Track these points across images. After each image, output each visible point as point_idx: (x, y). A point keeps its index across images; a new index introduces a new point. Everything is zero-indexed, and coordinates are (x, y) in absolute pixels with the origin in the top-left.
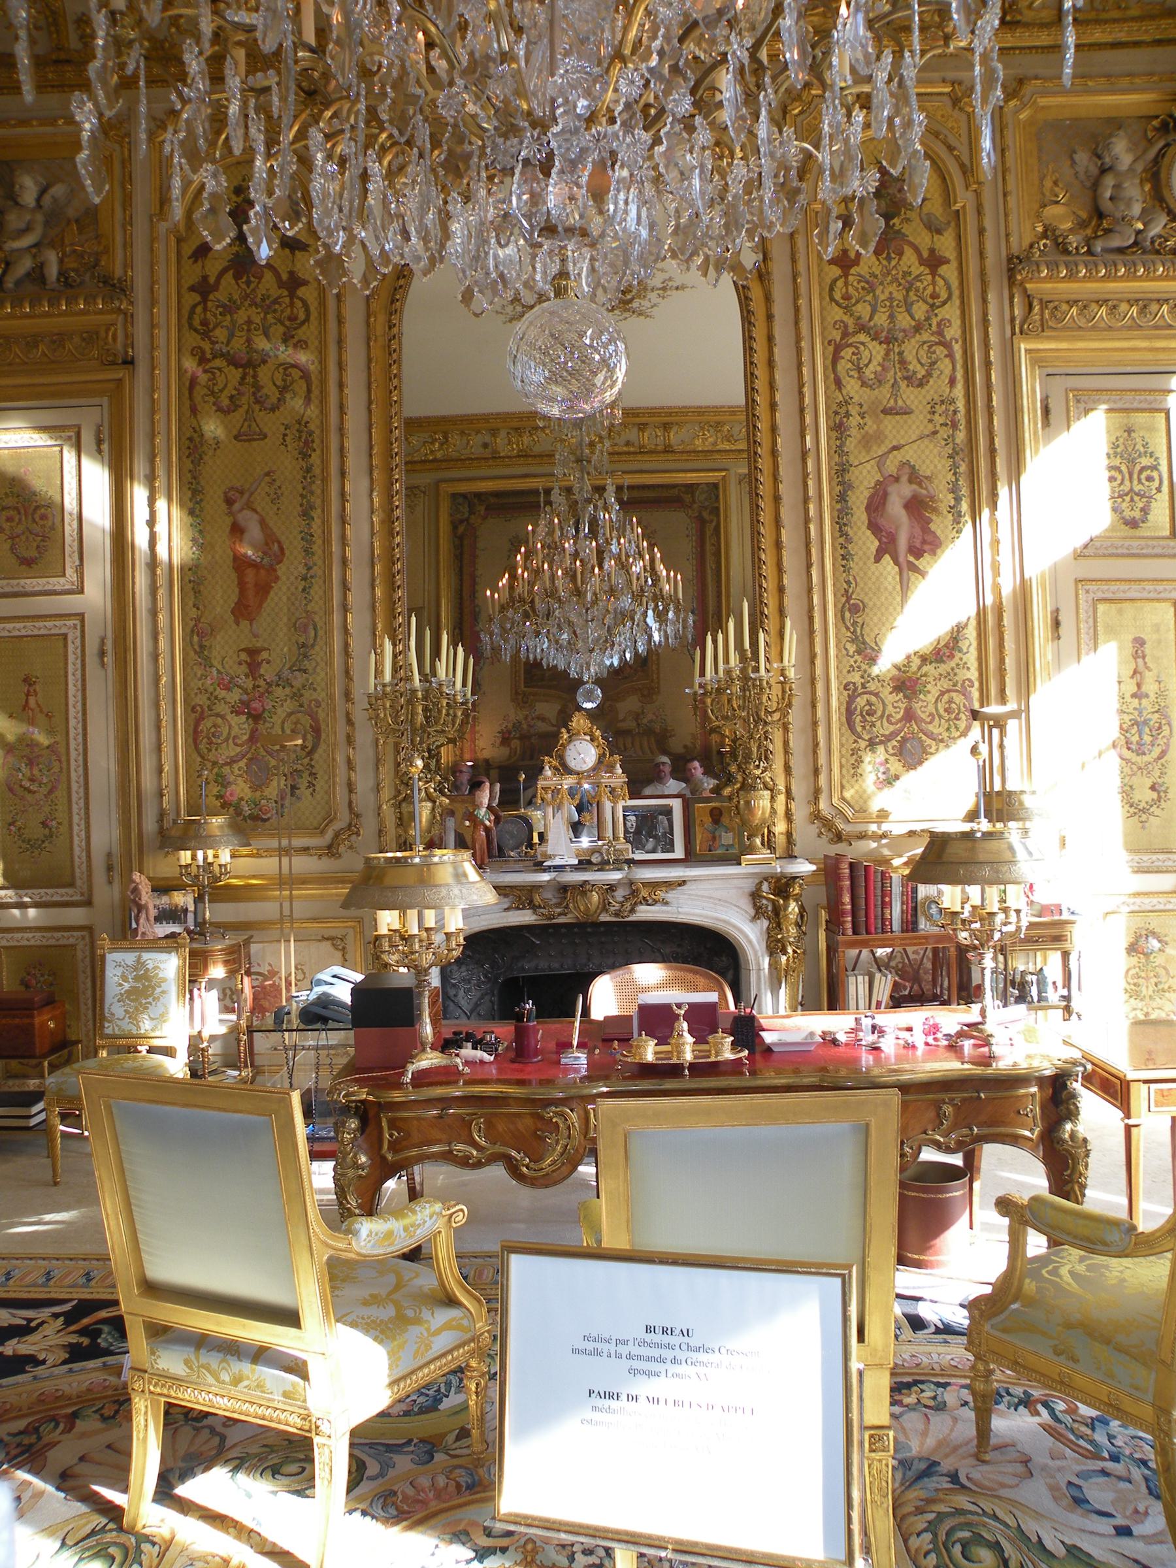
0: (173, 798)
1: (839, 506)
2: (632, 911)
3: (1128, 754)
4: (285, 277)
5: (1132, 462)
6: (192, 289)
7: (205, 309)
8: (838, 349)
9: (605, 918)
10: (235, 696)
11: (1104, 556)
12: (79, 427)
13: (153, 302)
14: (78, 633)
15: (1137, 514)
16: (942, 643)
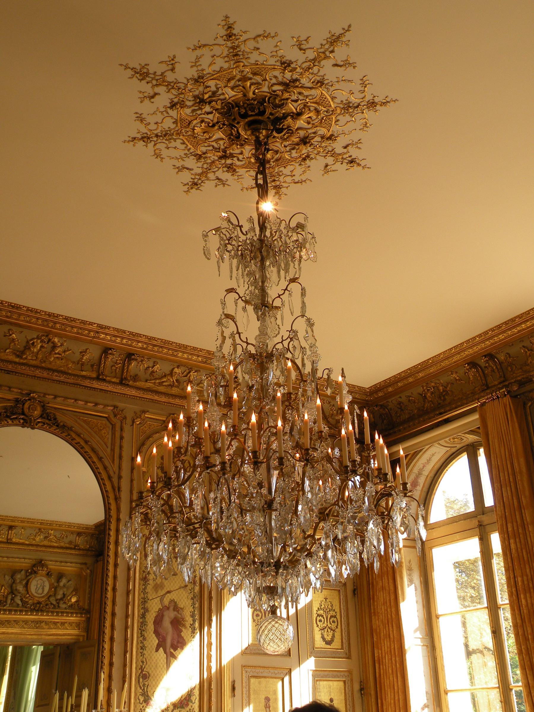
1: (141, 620)
11: (254, 654)
16: (184, 698)
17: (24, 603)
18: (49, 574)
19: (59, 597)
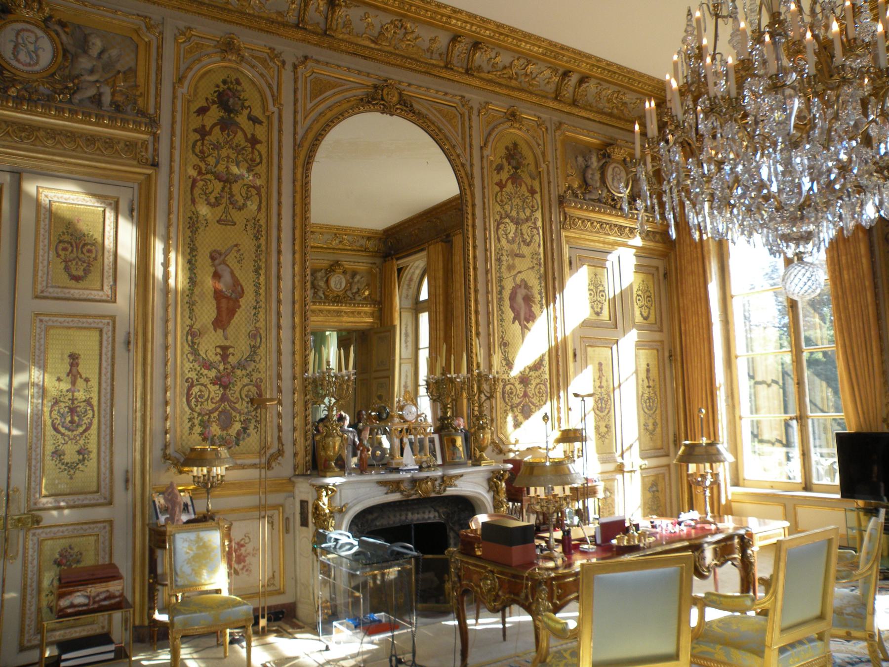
2: (445, 490)
3: (598, 412)
4: (249, 136)
5: (597, 288)
6: (195, 130)
7: (203, 144)
8: (498, 225)
9: (433, 495)
10: (213, 374)
14: (110, 328)
15: (599, 310)
17: (326, 297)
18: (344, 272)
19: (354, 291)
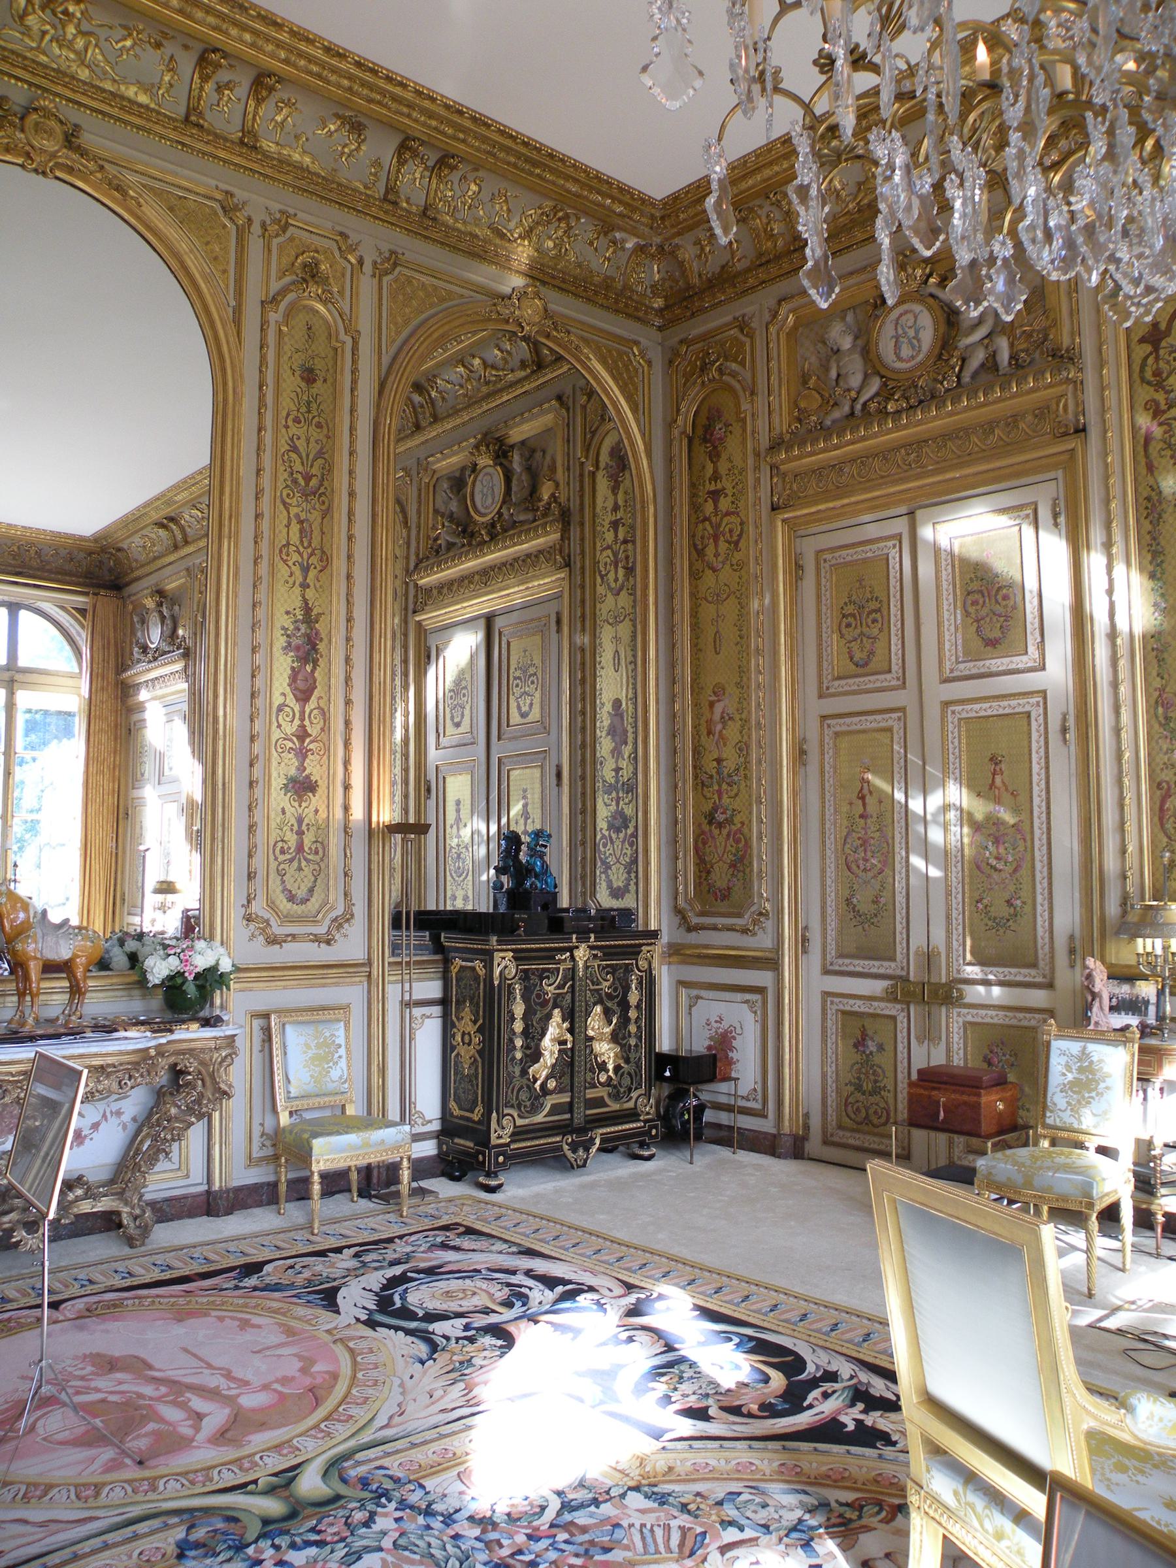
0: (1137, 880)
6: (1142, 340)
7: (1157, 359)
12: (1036, 503)
13: (1101, 364)
14: (1041, 710)
